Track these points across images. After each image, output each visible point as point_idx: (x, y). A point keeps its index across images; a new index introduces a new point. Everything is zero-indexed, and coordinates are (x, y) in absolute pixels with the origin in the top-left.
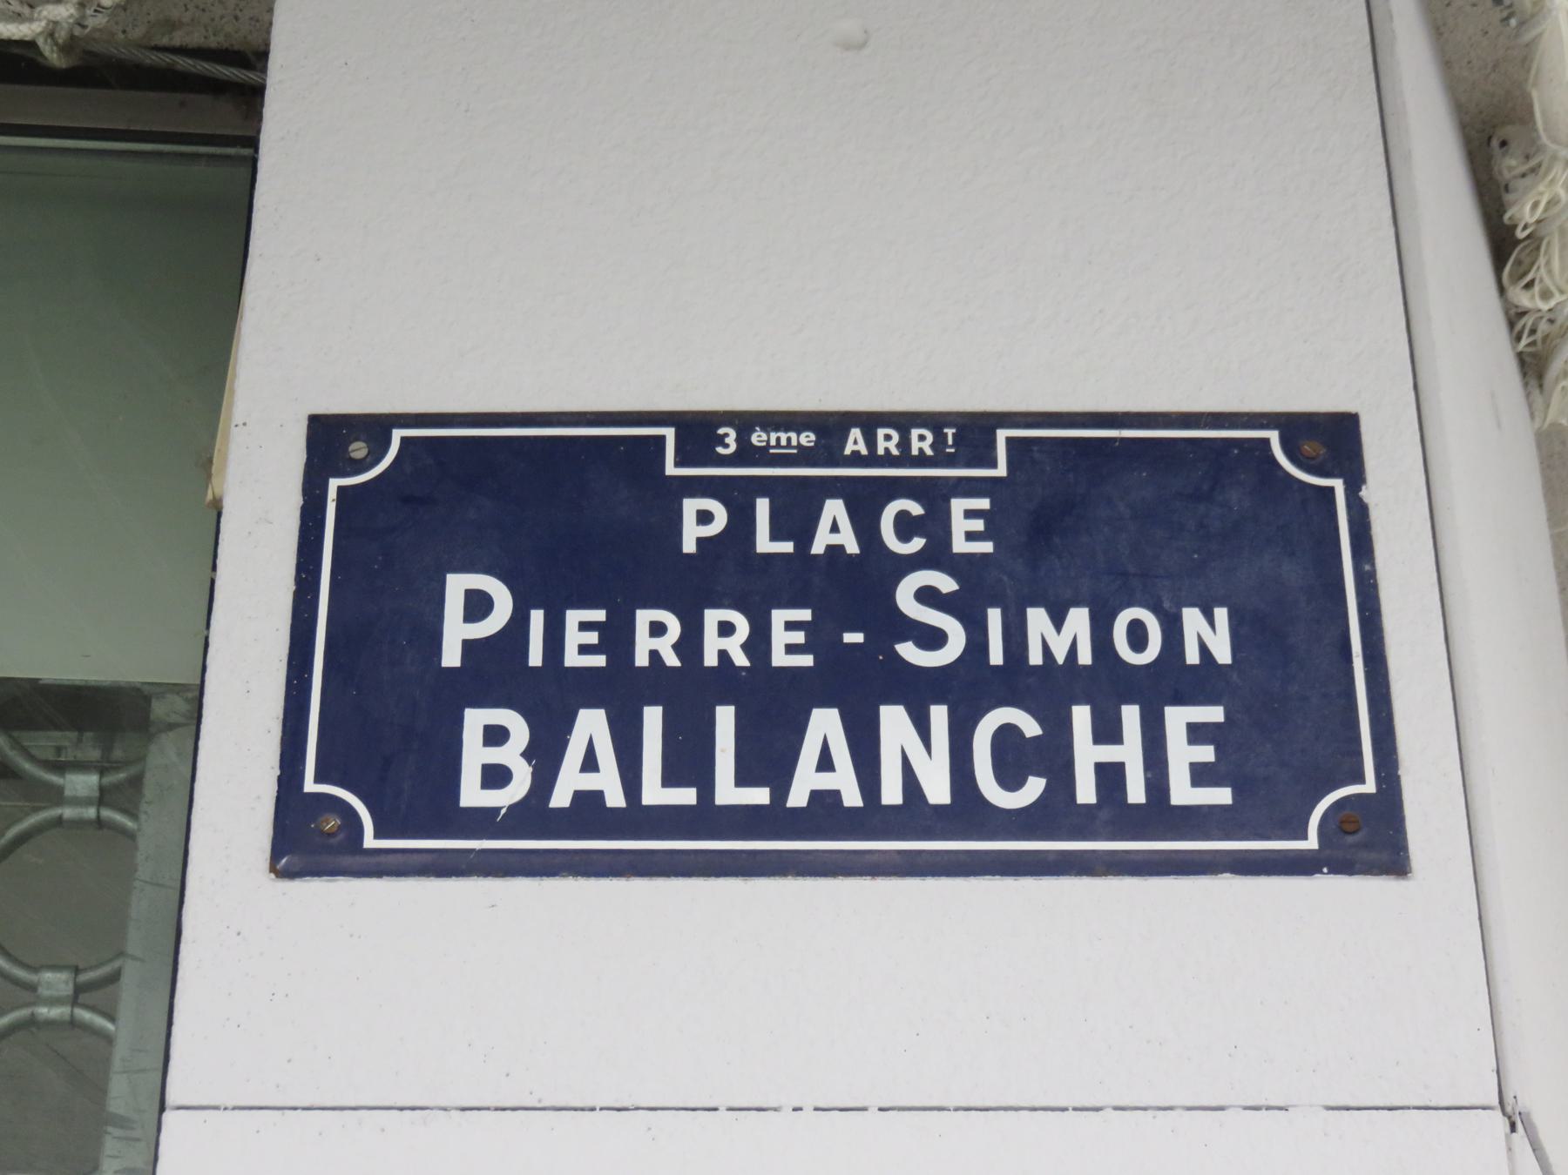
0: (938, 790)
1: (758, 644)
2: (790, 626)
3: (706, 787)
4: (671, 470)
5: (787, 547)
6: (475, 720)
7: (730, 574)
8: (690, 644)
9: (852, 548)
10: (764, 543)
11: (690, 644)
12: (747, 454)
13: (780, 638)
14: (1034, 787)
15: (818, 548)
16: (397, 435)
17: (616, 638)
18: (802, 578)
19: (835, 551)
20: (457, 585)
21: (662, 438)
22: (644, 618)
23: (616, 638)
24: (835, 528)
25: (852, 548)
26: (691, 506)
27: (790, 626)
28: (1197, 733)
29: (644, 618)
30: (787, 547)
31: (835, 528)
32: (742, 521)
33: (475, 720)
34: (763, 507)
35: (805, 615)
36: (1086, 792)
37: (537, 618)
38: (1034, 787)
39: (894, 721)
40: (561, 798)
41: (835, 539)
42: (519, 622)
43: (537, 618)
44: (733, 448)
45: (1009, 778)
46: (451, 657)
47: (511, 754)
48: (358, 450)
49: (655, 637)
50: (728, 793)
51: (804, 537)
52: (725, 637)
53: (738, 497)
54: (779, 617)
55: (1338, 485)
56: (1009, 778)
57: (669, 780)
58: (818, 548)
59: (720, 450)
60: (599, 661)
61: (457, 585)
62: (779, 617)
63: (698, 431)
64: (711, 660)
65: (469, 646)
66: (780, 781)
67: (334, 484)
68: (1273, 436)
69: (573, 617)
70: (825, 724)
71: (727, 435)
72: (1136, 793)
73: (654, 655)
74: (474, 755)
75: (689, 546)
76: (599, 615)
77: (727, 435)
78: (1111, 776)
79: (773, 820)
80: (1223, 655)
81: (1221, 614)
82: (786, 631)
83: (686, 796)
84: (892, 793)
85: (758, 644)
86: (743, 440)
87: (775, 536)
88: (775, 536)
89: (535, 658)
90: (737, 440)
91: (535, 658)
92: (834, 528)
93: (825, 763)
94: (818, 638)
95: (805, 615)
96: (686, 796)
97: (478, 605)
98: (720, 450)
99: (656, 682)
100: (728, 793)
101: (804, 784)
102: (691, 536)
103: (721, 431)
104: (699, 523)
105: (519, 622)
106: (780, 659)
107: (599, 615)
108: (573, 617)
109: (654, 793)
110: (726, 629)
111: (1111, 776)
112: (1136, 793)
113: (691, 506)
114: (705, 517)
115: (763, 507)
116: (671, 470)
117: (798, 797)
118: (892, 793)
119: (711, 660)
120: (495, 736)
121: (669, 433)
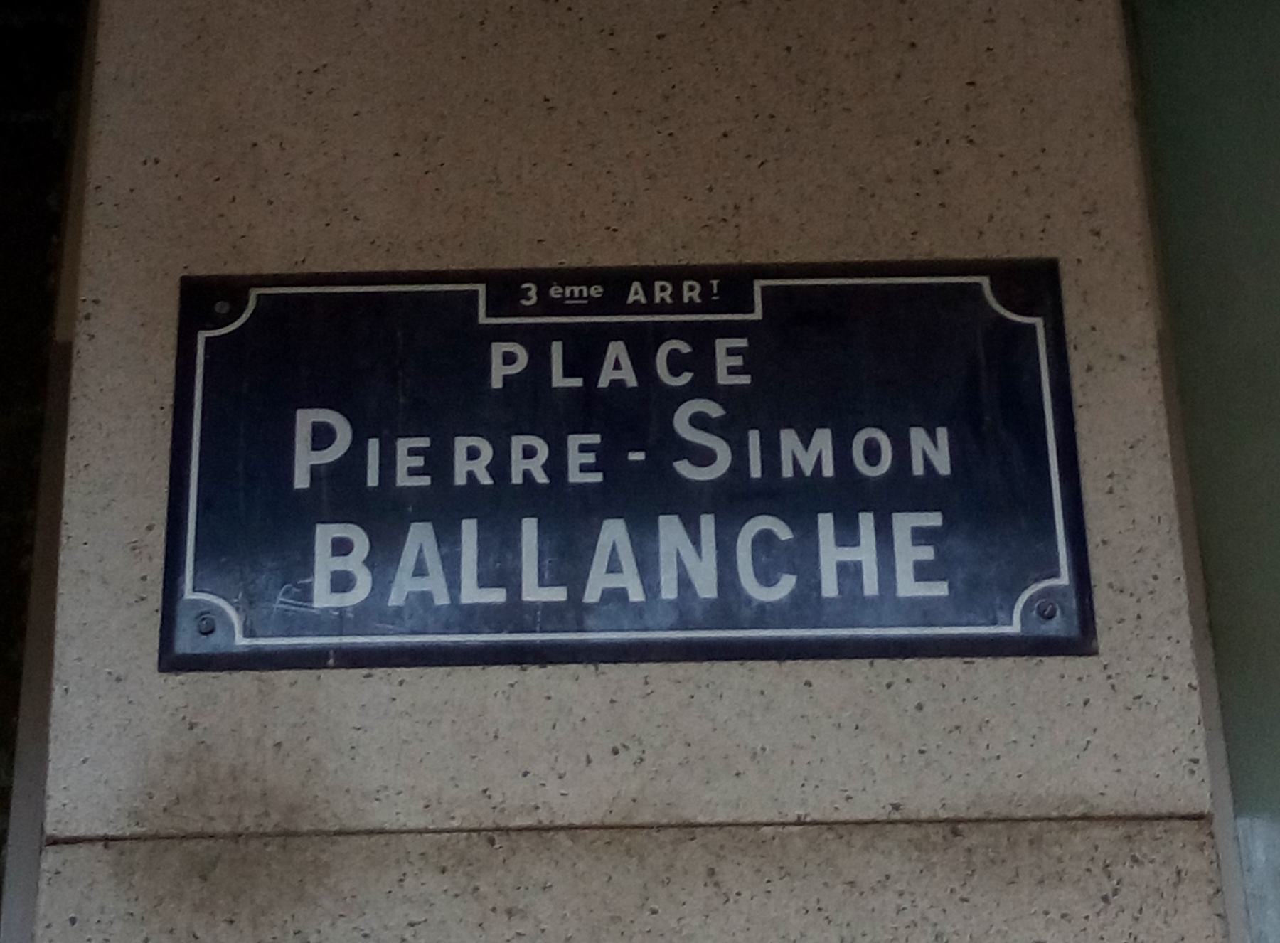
0: (707, 588)
1: (556, 466)
2: (584, 449)
3: (515, 589)
4: (483, 319)
5: (577, 382)
6: (325, 534)
7: (529, 406)
8: (500, 467)
9: (632, 381)
10: (559, 380)
11: (500, 467)
12: (547, 306)
13: (575, 459)
14: (787, 584)
15: (603, 383)
16: (254, 293)
17: (438, 462)
18: (591, 408)
19: (617, 385)
20: (305, 419)
21: (476, 292)
22: (461, 444)
23: (438, 462)
24: (617, 366)
25: (632, 381)
26: (498, 349)
27: (584, 449)
28: (920, 536)
29: (461, 444)
30: (577, 382)
31: (617, 366)
32: (540, 361)
33: (325, 534)
34: (557, 349)
35: (595, 439)
36: (830, 588)
37: (373, 445)
38: (787, 584)
39: (670, 529)
40: (396, 599)
41: (617, 375)
42: (357, 450)
43: (373, 445)
44: (534, 300)
45: (766, 578)
46: (301, 481)
47: (354, 562)
48: (221, 308)
49: (471, 461)
50: (533, 592)
51: (591, 375)
52: (529, 460)
53: (537, 341)
54: (574, 441)
55: (1038, 322)
56: (766, 578)
57: (483, 582)
58: (603, 383)
59: (524, 302)
60: (425, 481)
61: (305, 419)
62: (574, 441)
63: (504, 288)
64: (517, 479)
65: (315, 471)
66: (576, 584)
67: (202, 336)
68: (985, 281)
69: (403, 445)
70: (614, 533)
71: (529, 289)
72: (871, 586)
73: (471, 476)
74: (324, 564)
75: (497, 383)
76: (424, 442)
77: (529, 289)
78: (850, 573)
79: (574, 612)
80: (943, 466)
81: (942, 433)
82: (580, 452)
83: (497, 596)
84: (669, 591)
85: (556, 466)
86: (542, 293)
87: (567, 374)
88: (567, 374)
89: (373, 480)
90: (538, 294)
91: (373, 480)
92: (618, 367)
93: (614, 567)
94: (606, 459)
95: (595, 439)
96: (497, 596)
97: (322, 437)
98: (524, 302)
99: (471, 500)
100: (533, 592)
101: (597, 584)
102: (498, 374)
103: (525, 286)
104: (504, 364)
105: (357, 450)
106: (575, 477)
107: (424, 442)
108: (403, 445)
109: (471, 594)
110: (529, 453)
111: (850, 573)
112: (871, 586)
113: (498, 349)
114: (509, 359)
115: (557, 349)
116: (483, 319)
117: (592, 595)
118: (669, 591)
119: (517, 479)
120: (342, 547)
121: (481, 289)
